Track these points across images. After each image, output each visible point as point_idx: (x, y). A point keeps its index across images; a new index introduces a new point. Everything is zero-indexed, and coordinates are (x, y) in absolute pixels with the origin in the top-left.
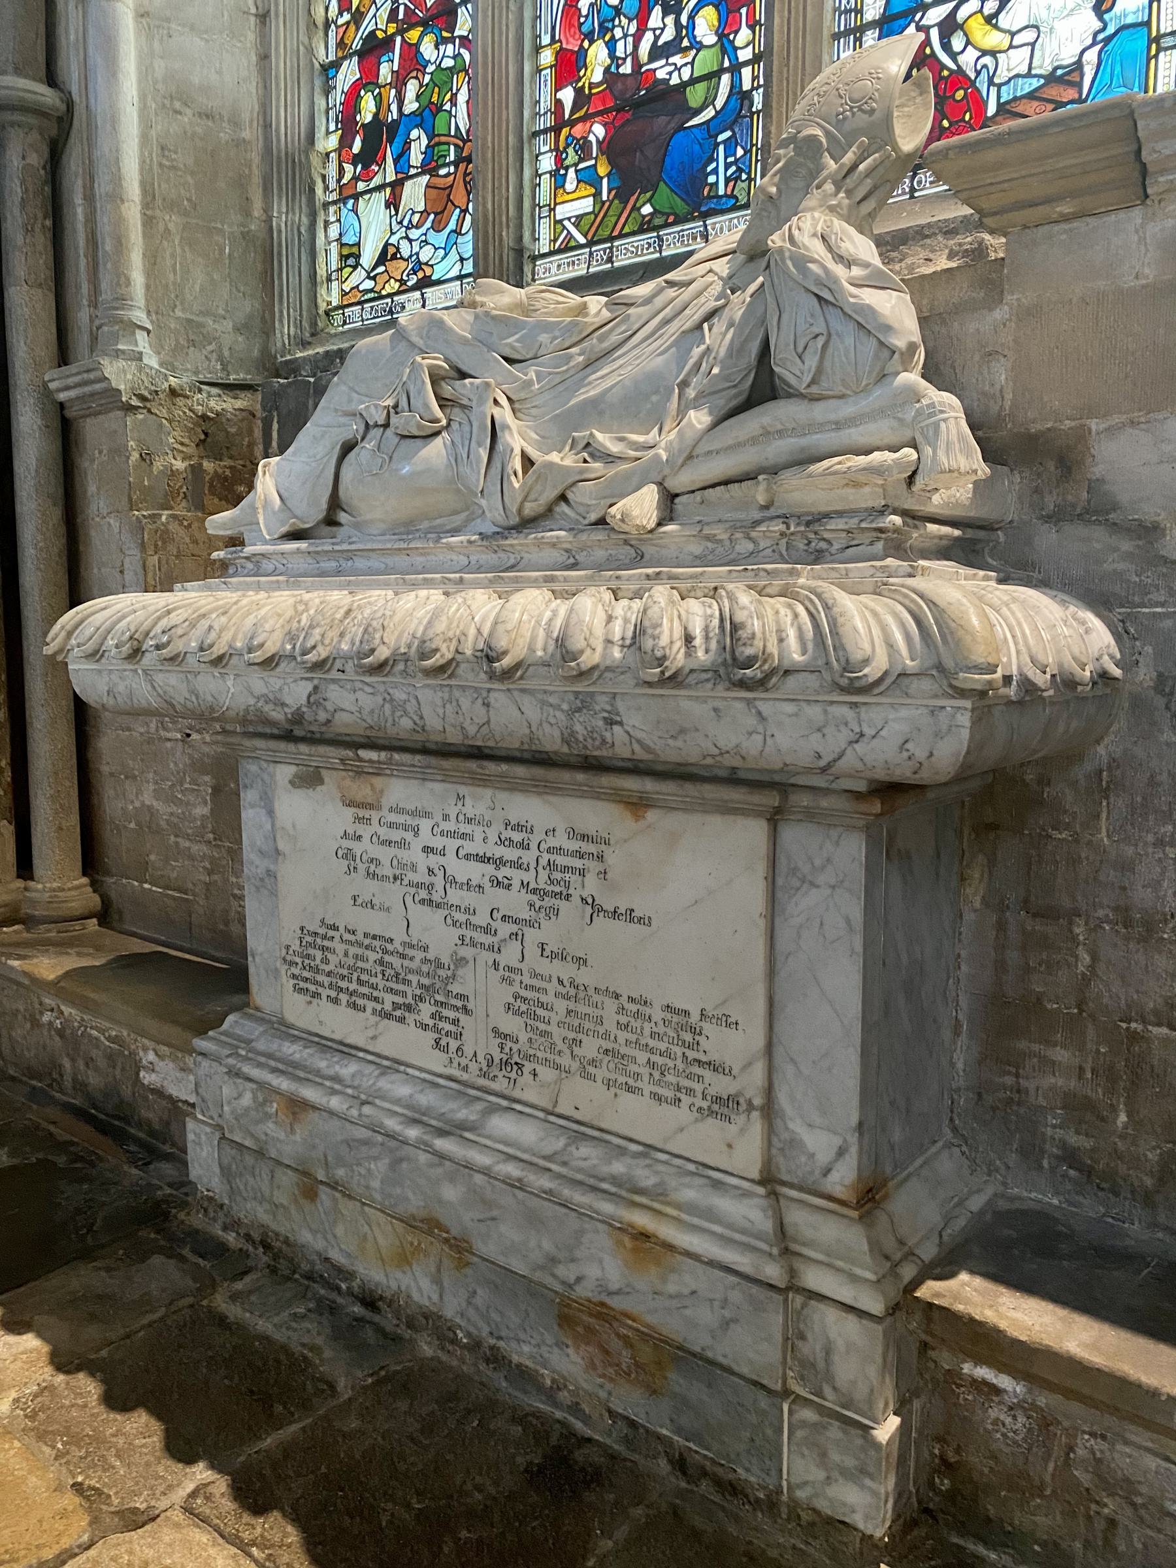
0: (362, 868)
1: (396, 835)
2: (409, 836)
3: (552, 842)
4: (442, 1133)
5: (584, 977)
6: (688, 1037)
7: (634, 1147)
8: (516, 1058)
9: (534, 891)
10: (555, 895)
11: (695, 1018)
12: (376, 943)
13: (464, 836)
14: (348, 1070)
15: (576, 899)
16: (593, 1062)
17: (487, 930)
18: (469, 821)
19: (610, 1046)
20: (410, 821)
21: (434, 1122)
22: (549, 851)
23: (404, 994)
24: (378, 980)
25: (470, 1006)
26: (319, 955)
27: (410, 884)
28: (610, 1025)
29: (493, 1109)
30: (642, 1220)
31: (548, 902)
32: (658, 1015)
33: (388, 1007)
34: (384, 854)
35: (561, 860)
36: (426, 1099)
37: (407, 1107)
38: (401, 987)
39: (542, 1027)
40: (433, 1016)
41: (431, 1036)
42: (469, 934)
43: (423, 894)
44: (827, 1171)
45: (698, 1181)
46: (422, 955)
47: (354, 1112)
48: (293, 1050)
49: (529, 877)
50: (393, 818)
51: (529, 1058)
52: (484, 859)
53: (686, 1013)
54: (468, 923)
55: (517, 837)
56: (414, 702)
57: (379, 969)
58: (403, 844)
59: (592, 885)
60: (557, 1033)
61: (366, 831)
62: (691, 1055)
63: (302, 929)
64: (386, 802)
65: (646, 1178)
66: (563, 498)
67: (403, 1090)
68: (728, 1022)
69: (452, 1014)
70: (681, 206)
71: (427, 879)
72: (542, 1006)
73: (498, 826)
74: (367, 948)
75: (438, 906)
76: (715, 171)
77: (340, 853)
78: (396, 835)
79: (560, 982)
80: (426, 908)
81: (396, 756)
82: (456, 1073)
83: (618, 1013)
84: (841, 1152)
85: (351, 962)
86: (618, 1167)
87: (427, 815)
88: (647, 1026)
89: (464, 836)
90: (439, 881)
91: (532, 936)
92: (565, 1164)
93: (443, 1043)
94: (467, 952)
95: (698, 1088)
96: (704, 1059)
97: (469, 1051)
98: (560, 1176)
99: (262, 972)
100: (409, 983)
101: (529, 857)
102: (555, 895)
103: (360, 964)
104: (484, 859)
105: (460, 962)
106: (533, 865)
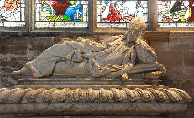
56: (97, 106)
66: (108, 74)
70: (69, 19)
76: (76, 15)
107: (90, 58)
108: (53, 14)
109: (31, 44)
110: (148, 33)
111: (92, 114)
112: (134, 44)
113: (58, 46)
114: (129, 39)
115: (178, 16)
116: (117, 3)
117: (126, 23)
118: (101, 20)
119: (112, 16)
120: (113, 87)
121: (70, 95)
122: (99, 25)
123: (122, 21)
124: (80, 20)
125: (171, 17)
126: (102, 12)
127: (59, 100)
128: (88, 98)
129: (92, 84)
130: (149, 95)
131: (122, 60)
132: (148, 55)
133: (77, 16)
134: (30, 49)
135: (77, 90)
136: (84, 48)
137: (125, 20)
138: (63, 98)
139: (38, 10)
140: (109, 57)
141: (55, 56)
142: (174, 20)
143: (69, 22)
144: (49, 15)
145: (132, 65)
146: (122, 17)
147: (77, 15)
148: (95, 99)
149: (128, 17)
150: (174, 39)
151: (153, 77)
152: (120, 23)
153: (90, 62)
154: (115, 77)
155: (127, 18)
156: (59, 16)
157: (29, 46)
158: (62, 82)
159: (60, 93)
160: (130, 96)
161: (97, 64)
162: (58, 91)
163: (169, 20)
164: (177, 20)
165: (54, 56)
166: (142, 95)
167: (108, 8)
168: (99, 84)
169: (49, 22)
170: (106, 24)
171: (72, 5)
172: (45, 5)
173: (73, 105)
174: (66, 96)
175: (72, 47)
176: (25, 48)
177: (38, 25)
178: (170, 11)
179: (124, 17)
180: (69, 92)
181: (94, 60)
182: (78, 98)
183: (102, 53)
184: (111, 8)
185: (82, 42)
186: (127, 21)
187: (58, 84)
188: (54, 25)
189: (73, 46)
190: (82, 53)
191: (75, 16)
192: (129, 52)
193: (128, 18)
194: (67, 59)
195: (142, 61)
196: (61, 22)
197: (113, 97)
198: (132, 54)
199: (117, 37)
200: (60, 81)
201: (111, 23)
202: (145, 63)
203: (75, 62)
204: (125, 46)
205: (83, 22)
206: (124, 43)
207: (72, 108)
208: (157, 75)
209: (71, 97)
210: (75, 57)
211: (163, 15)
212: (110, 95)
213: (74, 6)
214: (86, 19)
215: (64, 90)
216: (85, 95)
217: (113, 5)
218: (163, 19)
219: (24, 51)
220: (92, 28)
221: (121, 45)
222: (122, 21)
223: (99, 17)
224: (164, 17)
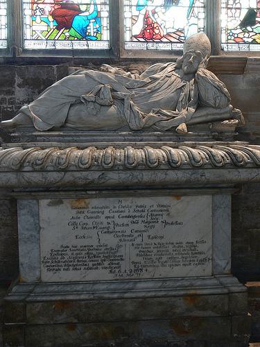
1: (95, 215)
3: (152, 209)
4: (125, 293)
5: (163, 241)
6: (193, 248)
14: (80, 288)
15: (160, 221)
16: (166, 262)
19: (169, 256)
24: (87, 259)
26: (60, 257)
28: (171, 251)
29: (136, 283)
30: (192, 292)
31: (151, 224)
32: (184, 245)
33: (91, 265)
34: (90, 222)
35: (155, 213)
36: (113, 286)
37: (108, 290)
41: (108, 270)
43: (106, 230)
44: (224, 269)
47: (92, 297)
48: (50, 289)
49: (145, 219)
50: (94, 210)
51: (144, 266)
52: (129, 217)
53: (192, 243)
55: (140, 209)
56: (141, 175)
57: (87, 255)
58: (98, 217)
59: (165, 217)
60: (154, 258)
63: (52, 250)
65: (186, 283)
66: (154, 124)
67: (105, 286)
68: (203, 242)
69: (116, 262)
70: (79, 37)
76: (90, 29)
78: (95, 215)
80: (107, 234)
81: (104, 192)
82: (118, 278)
84: (228, 263)
86: (179, 284)
88: (182, 249)
90: (112, 226)
91: (145, 234)
93: (113, 270)
97: (123, 270)
99: (27, 270)
101: (143, 214)
104: (129, 217)
105: (119, 246)
107: (126, 99)
108: (52, 27)
109: (22, 76)
110: (213, 58)
111: (130, 188)
112: (194, 77)
113: (69, 79)
114: (186, 68)
115: (251, 34)
116: (156, 10)
117: (171, 42)
118: (131, 38)
119: (148, 31)
120: (165, 144)
121: (99, 158)
122: (128, 46)
123: (164, 40)
124: (96, 37)
125: (241, 36)
126: (133, 24)
127: (81, 166)
128: (128, 163)
129: (130, 140)
130: (223, 157)
131: (177, 102)
132: (218, 94)
133: (91, 30)
134: (19, 86)
135: (109, 151)
136: (115, 82)
137: (169, 38)
138: (87, 163)
139: (27, 20)
140: (156, 97)
141: (69, 96)
142: (246, 40)
143: (80, 40)
144: (45, 28)
145: (192, 110)
146: (165, 34)
147: (92, 29)
148: (139, 164)
149: (174, 33)
150: (252, 69)
151: (226, 128)
152: (162, 42)
153: (126, 105)
154: (166, 129)
155: (172, 35)
156: (62, 30)
157: (18, 80)
158: (81, 138)
159: (82, 155)
160: (194, 159)
161: (136, 108)
162: (79, 153)
163: (238, 40)
164: (250, 40)
165: (65, 95)
166: (211, 156)
167: (141, 17)
168: (141, 141)
169: (47, 39)
170: (139, 43)
171: (83, 12)
172: (38, 11)
173: (103, 174)
175: (96, 81)
176: (12, 83)
177: (29, 45)
178: (240, 25)
179: (168, 34)
180: (96, 154)
181: (132, 102)
182: (112, 163)
183: (145, 90)
184: (146, 17)
185: (110, 72)
186: (173, 40)
187: (76, 141)
188: (54, 45)
189: (97, 79)
190: (113, 90)
191: (89, 31)
192: (186, 90)
193: (174, 35)
195: (207, 103)
196: (65, 40)
197: (166, 159)
198: (192, 92)
199: (166, 65)
200: (78, 136)
201: (148, 42)
202: (213, 107)
203: (101, 105)
204: (180, 80)
205: (101, 40)
206: (177, 75)
207: (101, 178)
208: (231, 125)
209: (100, 162)
210: (102, 96)
211: (229, 32)
212: (162, 157)
213: (87, 14)
214: (106, 35)
215: (87, 151)
216: (122, 158)
217: (150, 14)
218: (229, 37)
219: (10, 88)
220: (119, 51)
221: (173, 78)
222: (164, 40)
223: (128, 32)
224: (231, 34)
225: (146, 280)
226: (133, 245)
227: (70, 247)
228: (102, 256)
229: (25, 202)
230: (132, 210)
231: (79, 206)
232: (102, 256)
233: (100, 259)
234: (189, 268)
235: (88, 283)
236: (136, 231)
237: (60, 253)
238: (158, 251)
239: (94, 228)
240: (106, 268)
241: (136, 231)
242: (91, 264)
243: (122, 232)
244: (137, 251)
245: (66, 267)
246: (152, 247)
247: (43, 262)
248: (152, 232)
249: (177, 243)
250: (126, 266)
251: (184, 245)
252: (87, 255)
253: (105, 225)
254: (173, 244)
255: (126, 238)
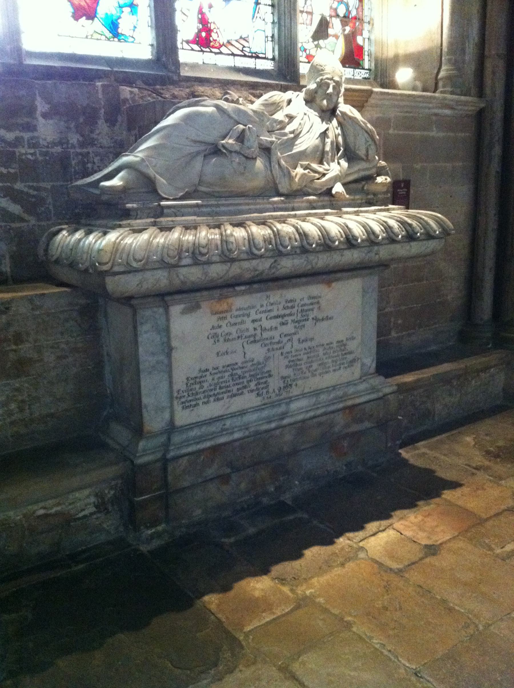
0: (221, 339)
1: (239, 320)
2: (245, 318)
3: (302, 303)
4: (283, 419)
5: (313, 344)
7: (330, 389)
8: (290, 383)
9: (297, 322)
10: (304, 320)
11: (344, 342)
12: (229, 368)
13: (269, 311)
15: (310, 318)
16: (316, 370)
17: (279, 342)
18: (272, 304)
19: (320, 362)
20: (246, 312)
21: (276, 418)
22: (302, 306)
23: (243, 382)
24: (231, 383)
25: (271, 373)
26: (197, 386)
27: (246, 337)
29: (288, 404)
30: (350, 403)
33: (235, 391)
34: (233, 330)
35: (305, 308)
36: (265, 413)
37: (260, 420)
38: (241, 381)
39: (299, 367)
40: (256, 385)
41: (255, 393)
42: (270, 347)
43: (252, 339)
45: (351, 386)
46: (251, 363)
50: (237, 313)
53: (342, 341)
54: (271, 343)
55: (290, 305)
56: (316, 259)
58: (243, 322)
59: (315, 313)
61: (223, 323)
62: (343, 353)
63: (188, 379)
64: (234, 308)
65: (340, 393)
68: (353, 338)
69: (264, 380)
71: (253, 332)
72: (299, 360)
73: (283, 303)
74: (224, 372)
75: (258, 341)
77: (210, 336)
78: (239, 320)
79: (305, 349)
82: (266, 401)
83: (324, 350)
85: (216, 381)
86: (332, 396)
87: (253, 307)
89: (269, 311)
90: (259, 332)
92: (319, 404)
93: (261, 393)
94: (271, 354)
95: (345, 361)
96: (347, 352)
97: (271, 390)
98: (323, 407)
100: (245, 377)
101: (294, 310)
102: (304, 320)
103: (221, 380)
106: (296, 312)
145: (344, 164)
151: (380, 189)
154: (319, 192)
158: (223, 209)
173: (275, 261)
174: (265, 242)
189: (233, 116)
192: (331, 134)
194: (232, 150)
195: (358, 155)
197: (344, 236)
200: (218, 206)
212: (338, 233)
225: (298, 398)
226: (282, 354)
227: (211, 370)
228: (247, 375)
229: (148, 313)
230: (281, 307)
231: (221, 309)
232: (247, 375)
233: (245, 380)
234: (337, 373)
235: (233, 415)
236: (285, 336)
237: (198, 380)
238: (308, 358)
239: (238, 337)
240: (252, 391)
241: (285, 336)
242: (235, 389)
243: (271, 338)
244: (286, 362)
245: (206, 400)
246: (302, 353)
247: (177, 398)
248: (302, 334)
249: (327, 344)
250: (274, 384)
251: (335, 345)
252: (230, 378)
253: (252, 332)
254: (323, 345)
255: (275, 346)
